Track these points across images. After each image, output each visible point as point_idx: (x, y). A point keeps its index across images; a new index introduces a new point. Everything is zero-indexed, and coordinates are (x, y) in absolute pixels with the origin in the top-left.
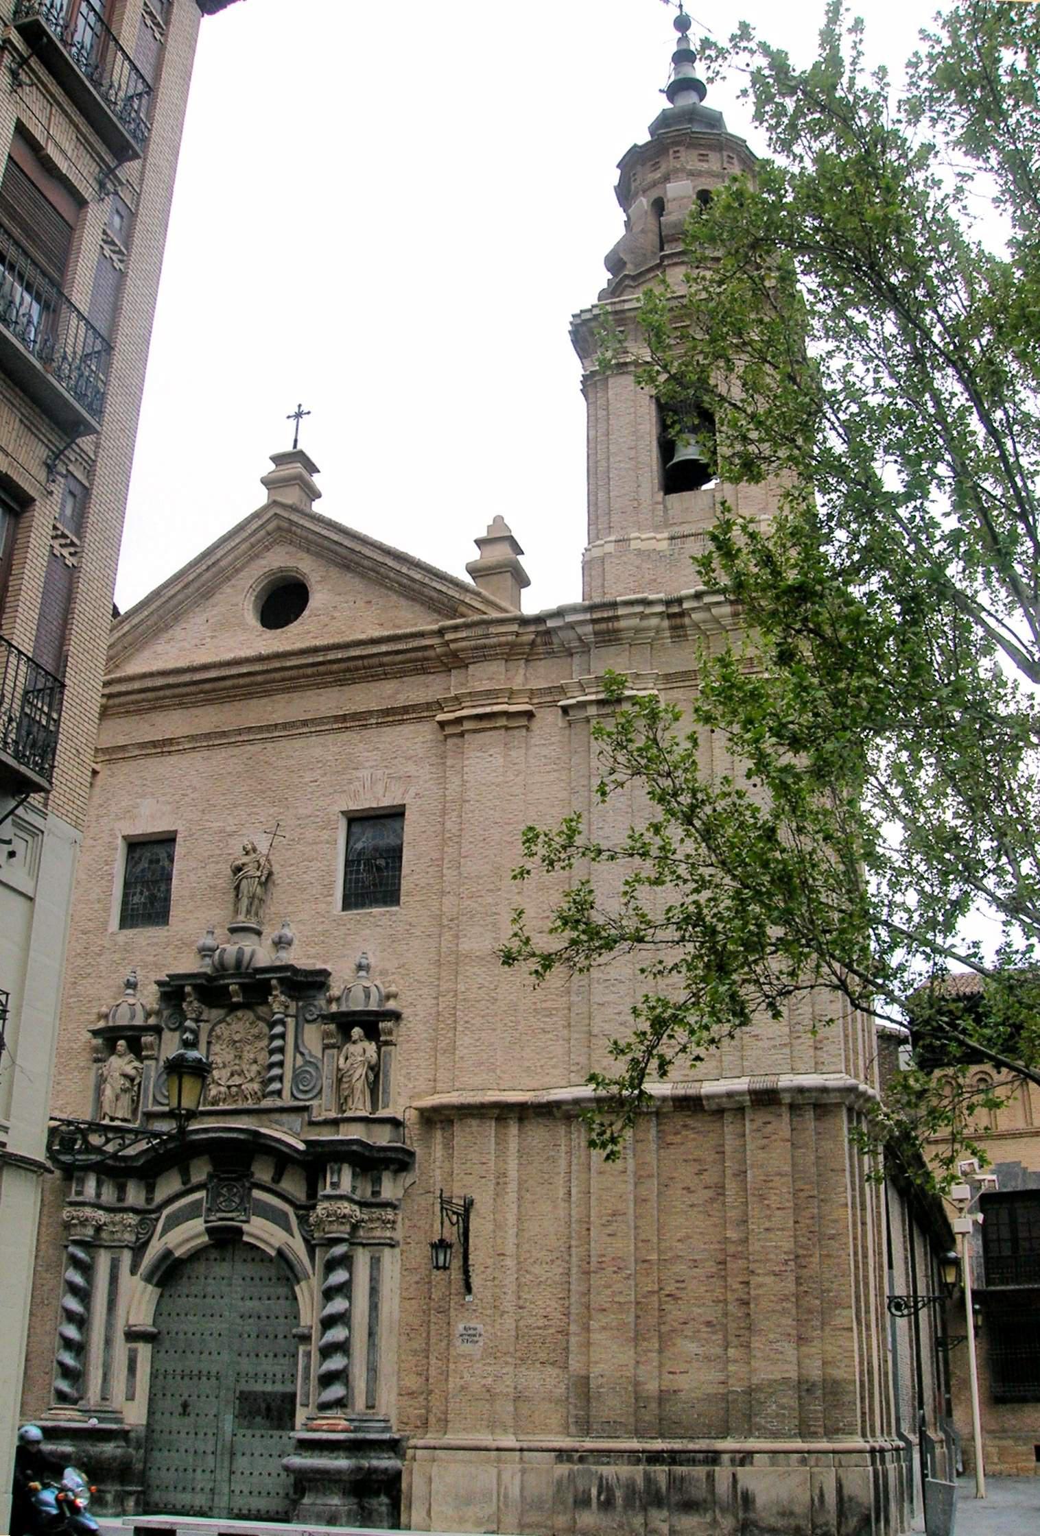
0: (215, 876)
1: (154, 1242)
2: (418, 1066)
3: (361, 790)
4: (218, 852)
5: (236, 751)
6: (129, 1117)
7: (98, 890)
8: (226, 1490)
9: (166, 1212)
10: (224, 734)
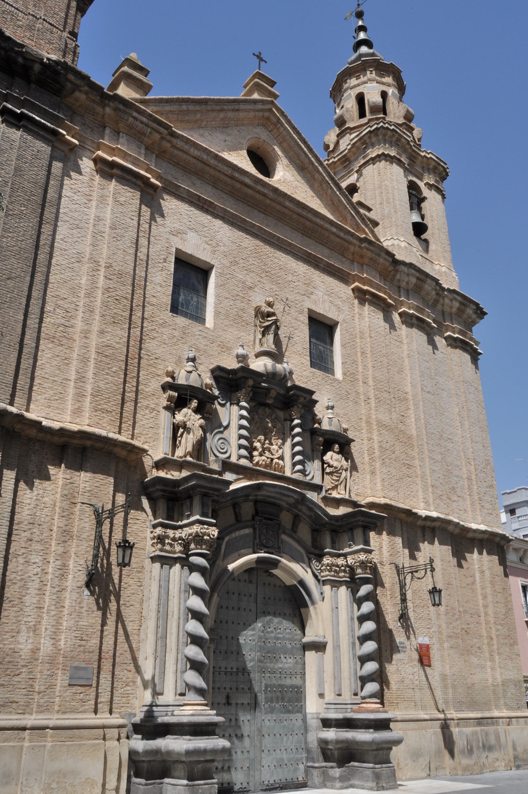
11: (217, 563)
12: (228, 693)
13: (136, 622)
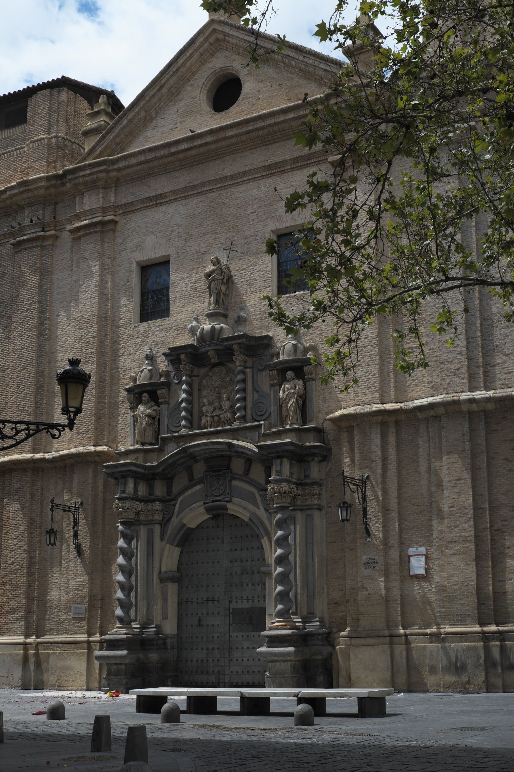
1: (174, 519)
4: (196, 266)
5: (203, 198)
6: (154, 442)
8: (227, 672)
9: (180, 499)
10: (194, 187)
11: (172, 520)
12: (200, 617)
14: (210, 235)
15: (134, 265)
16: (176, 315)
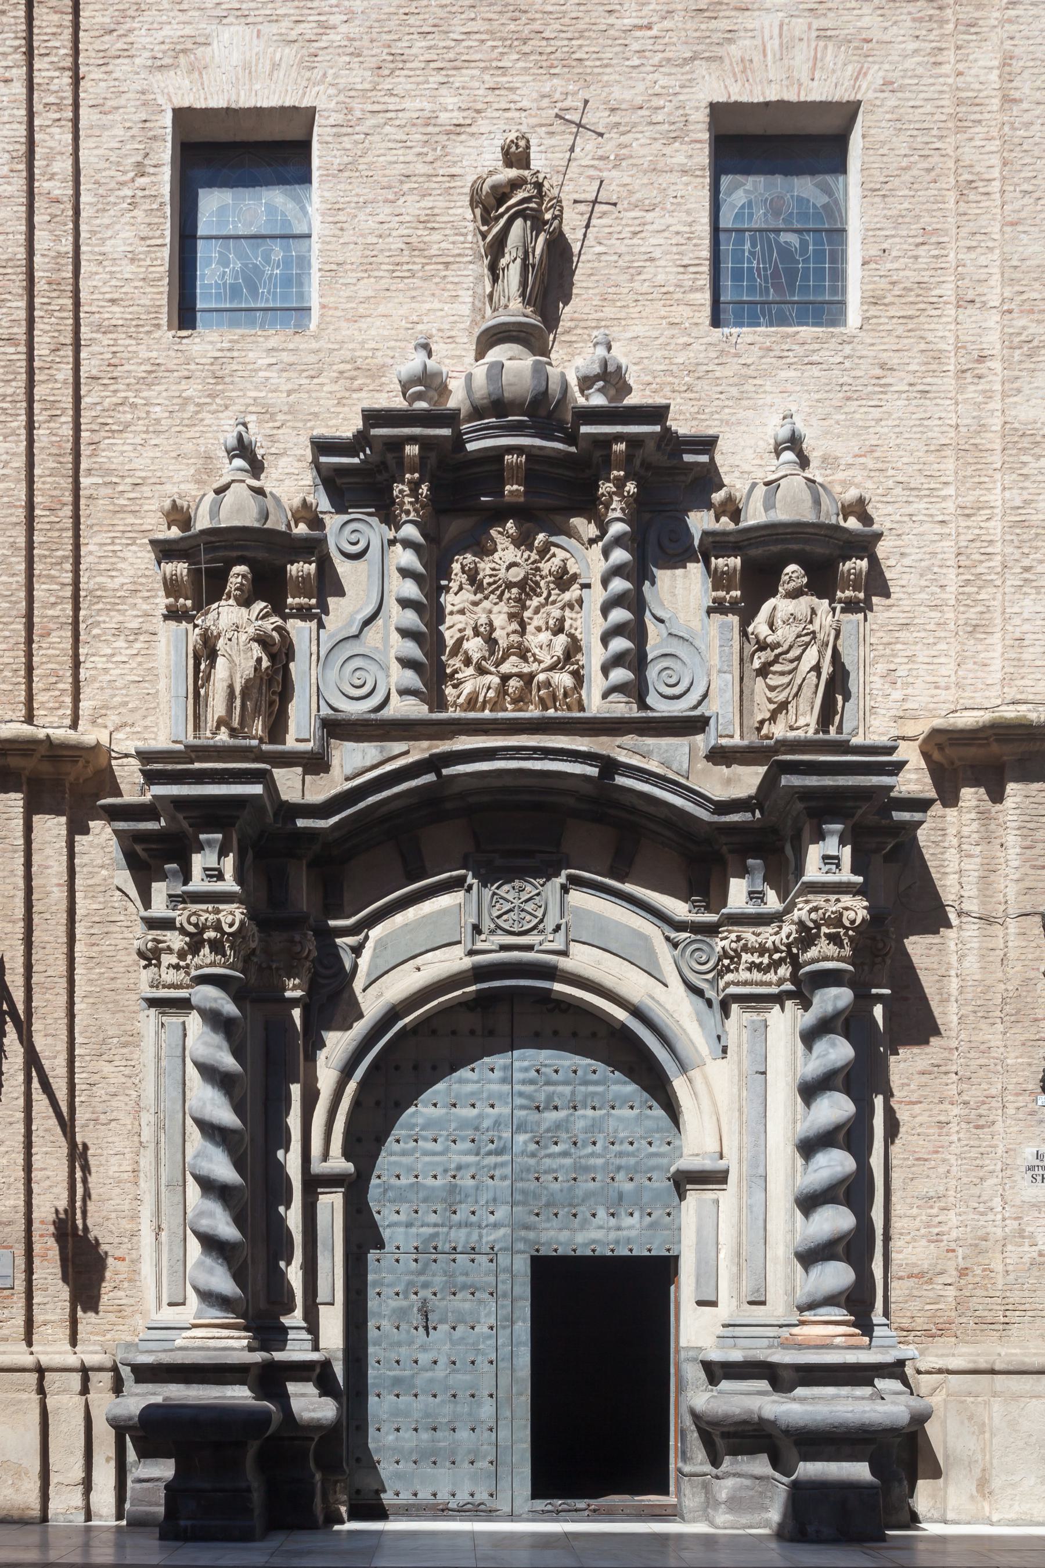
0: (427, 222)
2: (911, 658)
3: (757, 58)
4: (422, 168)
7: (128, 234)
13: (127, 1156)
14: (476, 72)
15: (168, 119)
16: (344, 324)
